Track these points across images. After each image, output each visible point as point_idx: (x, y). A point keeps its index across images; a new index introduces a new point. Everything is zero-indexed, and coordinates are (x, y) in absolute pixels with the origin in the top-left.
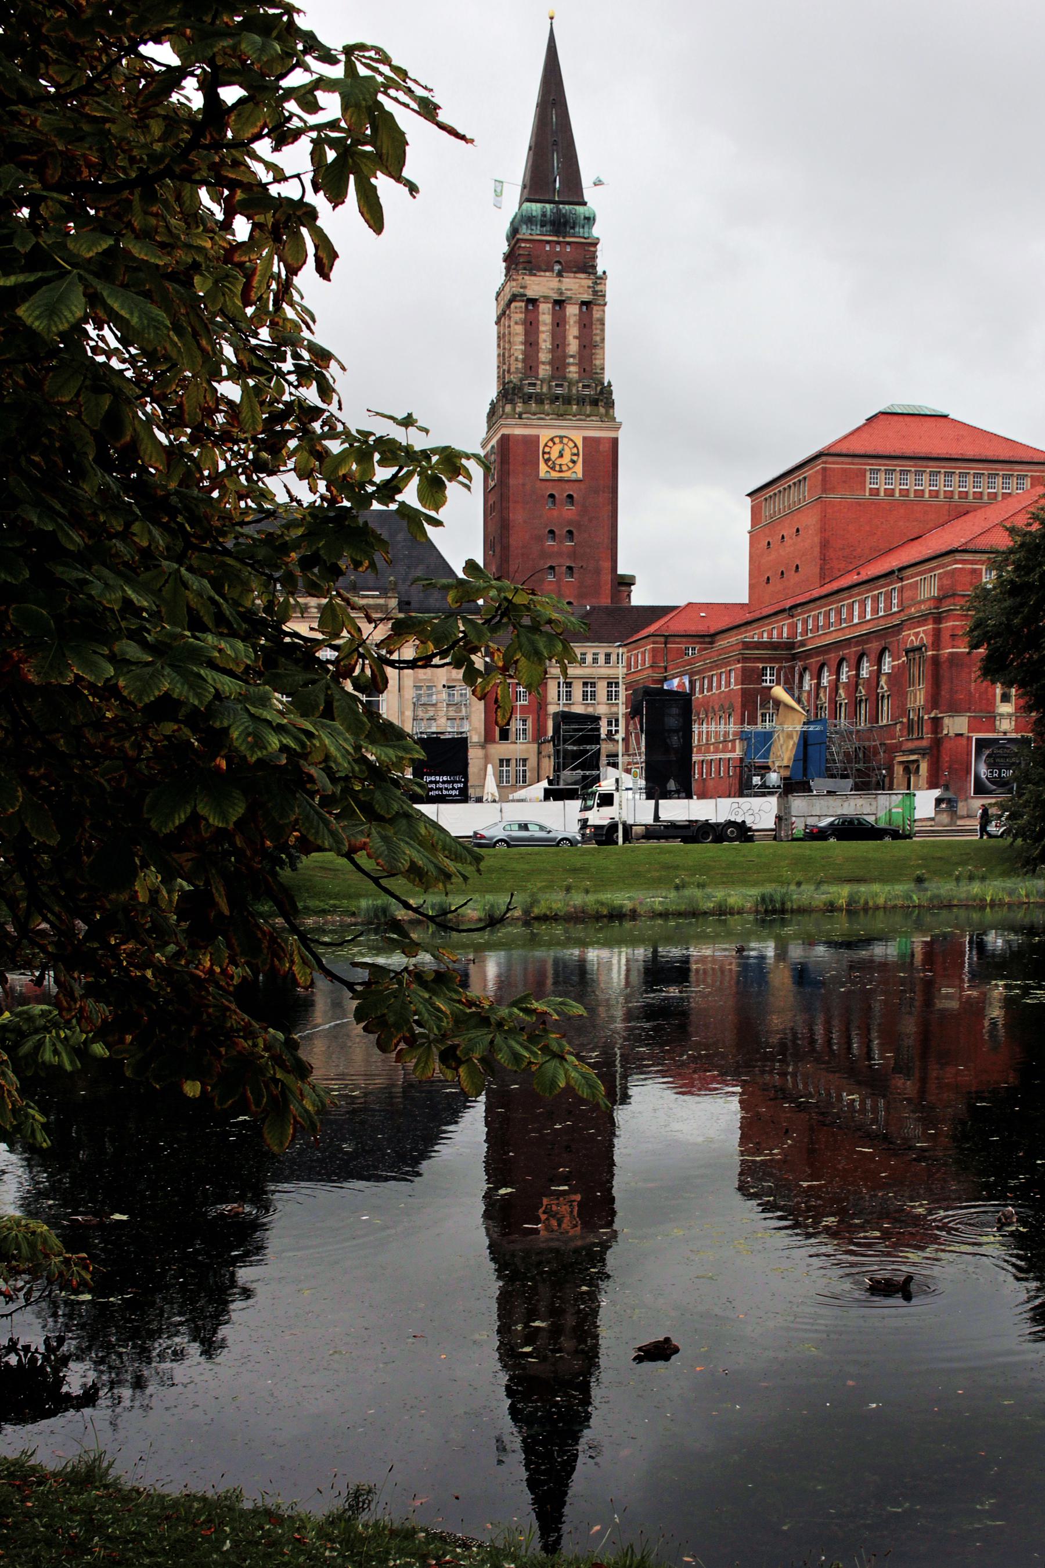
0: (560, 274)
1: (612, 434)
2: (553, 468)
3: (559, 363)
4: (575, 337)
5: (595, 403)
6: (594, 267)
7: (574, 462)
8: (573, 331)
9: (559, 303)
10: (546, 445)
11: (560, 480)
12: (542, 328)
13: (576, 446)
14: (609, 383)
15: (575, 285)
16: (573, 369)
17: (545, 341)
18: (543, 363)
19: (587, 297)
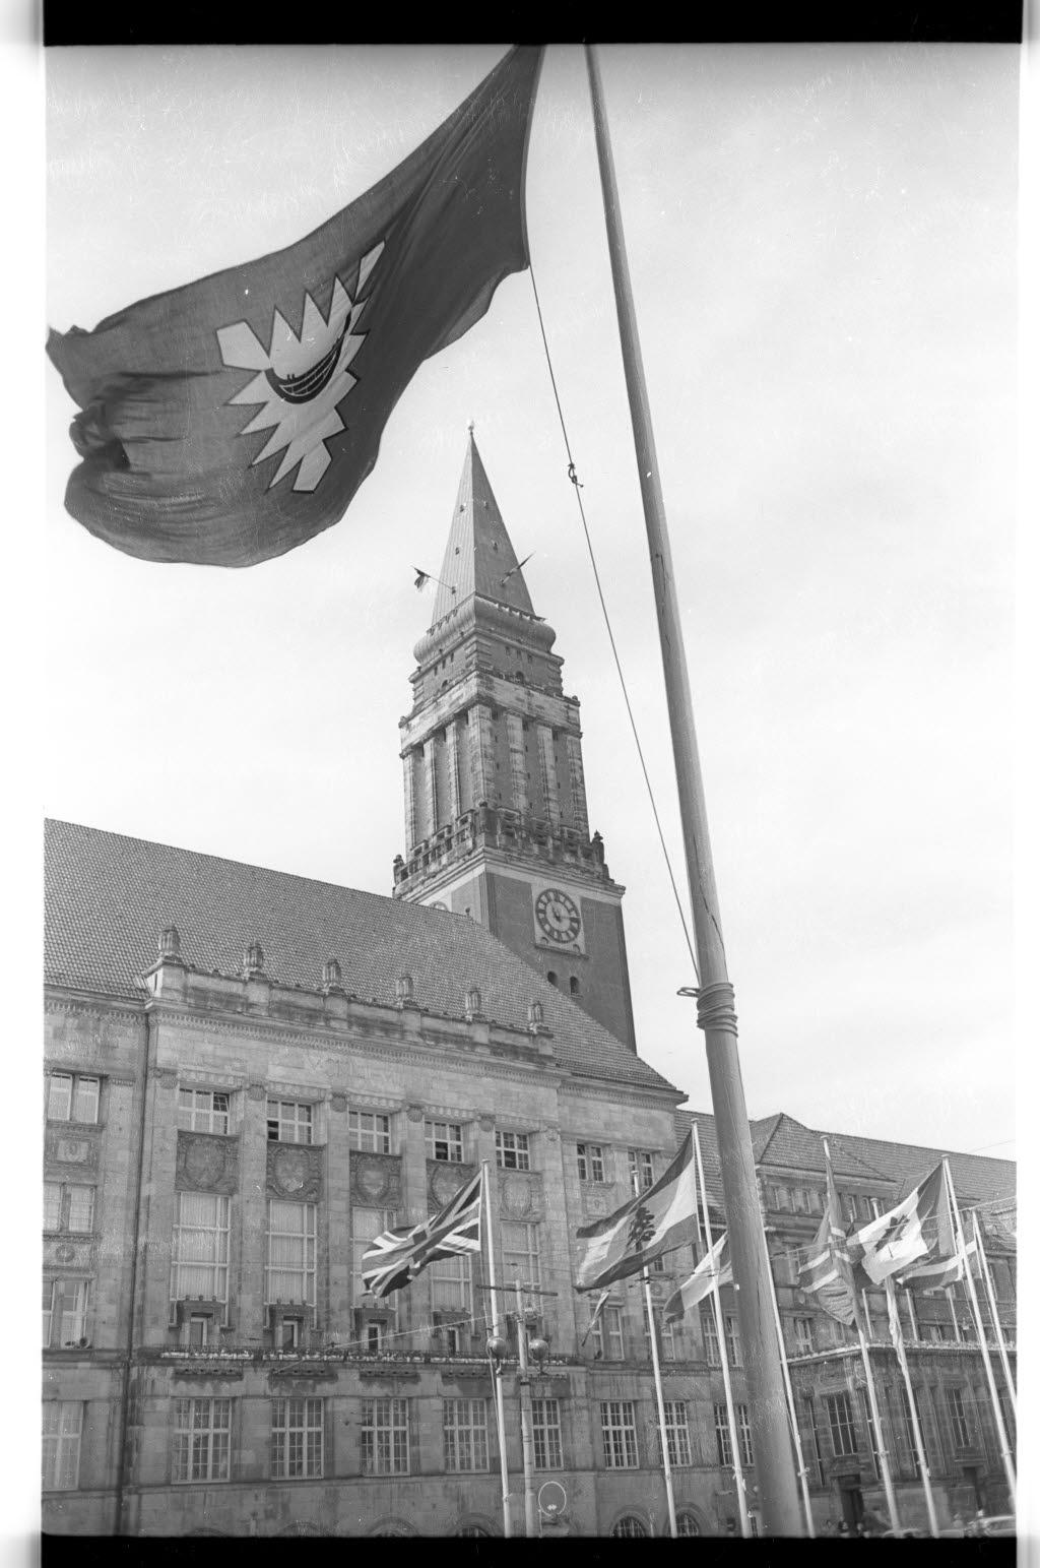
4: (552, 767)
10: (539, 900)
13: (574, 908)
14: (598, 837)
19: (559, 721)
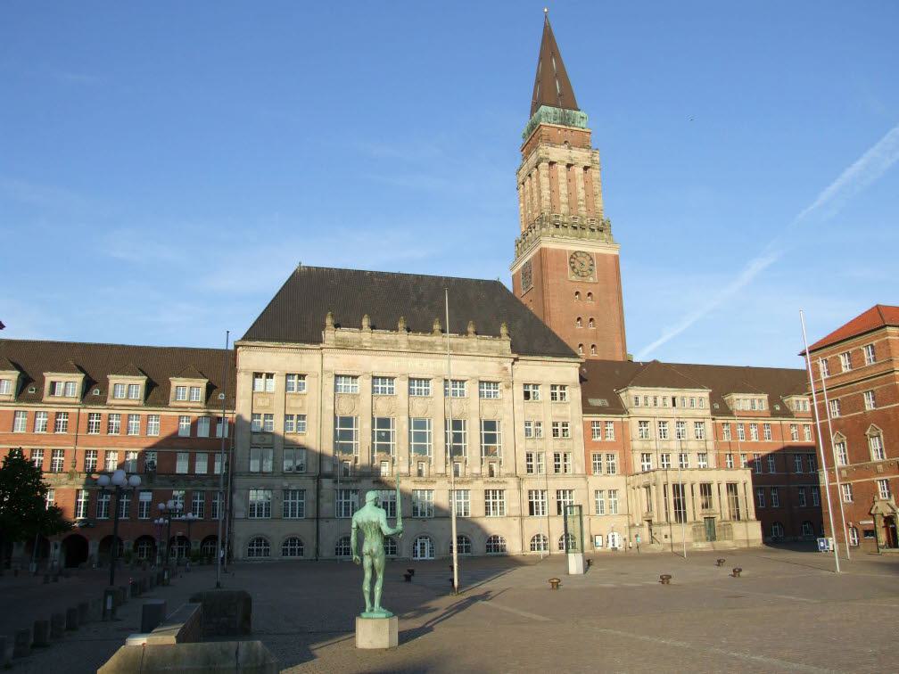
1: (616, 253)
3: (572, 204)
7: (591, 270)
10: (572, 257)
12: (561, 181)
13: (591, 259)
15: (580, 156)
18: (563, 203)
19: (588, 164)
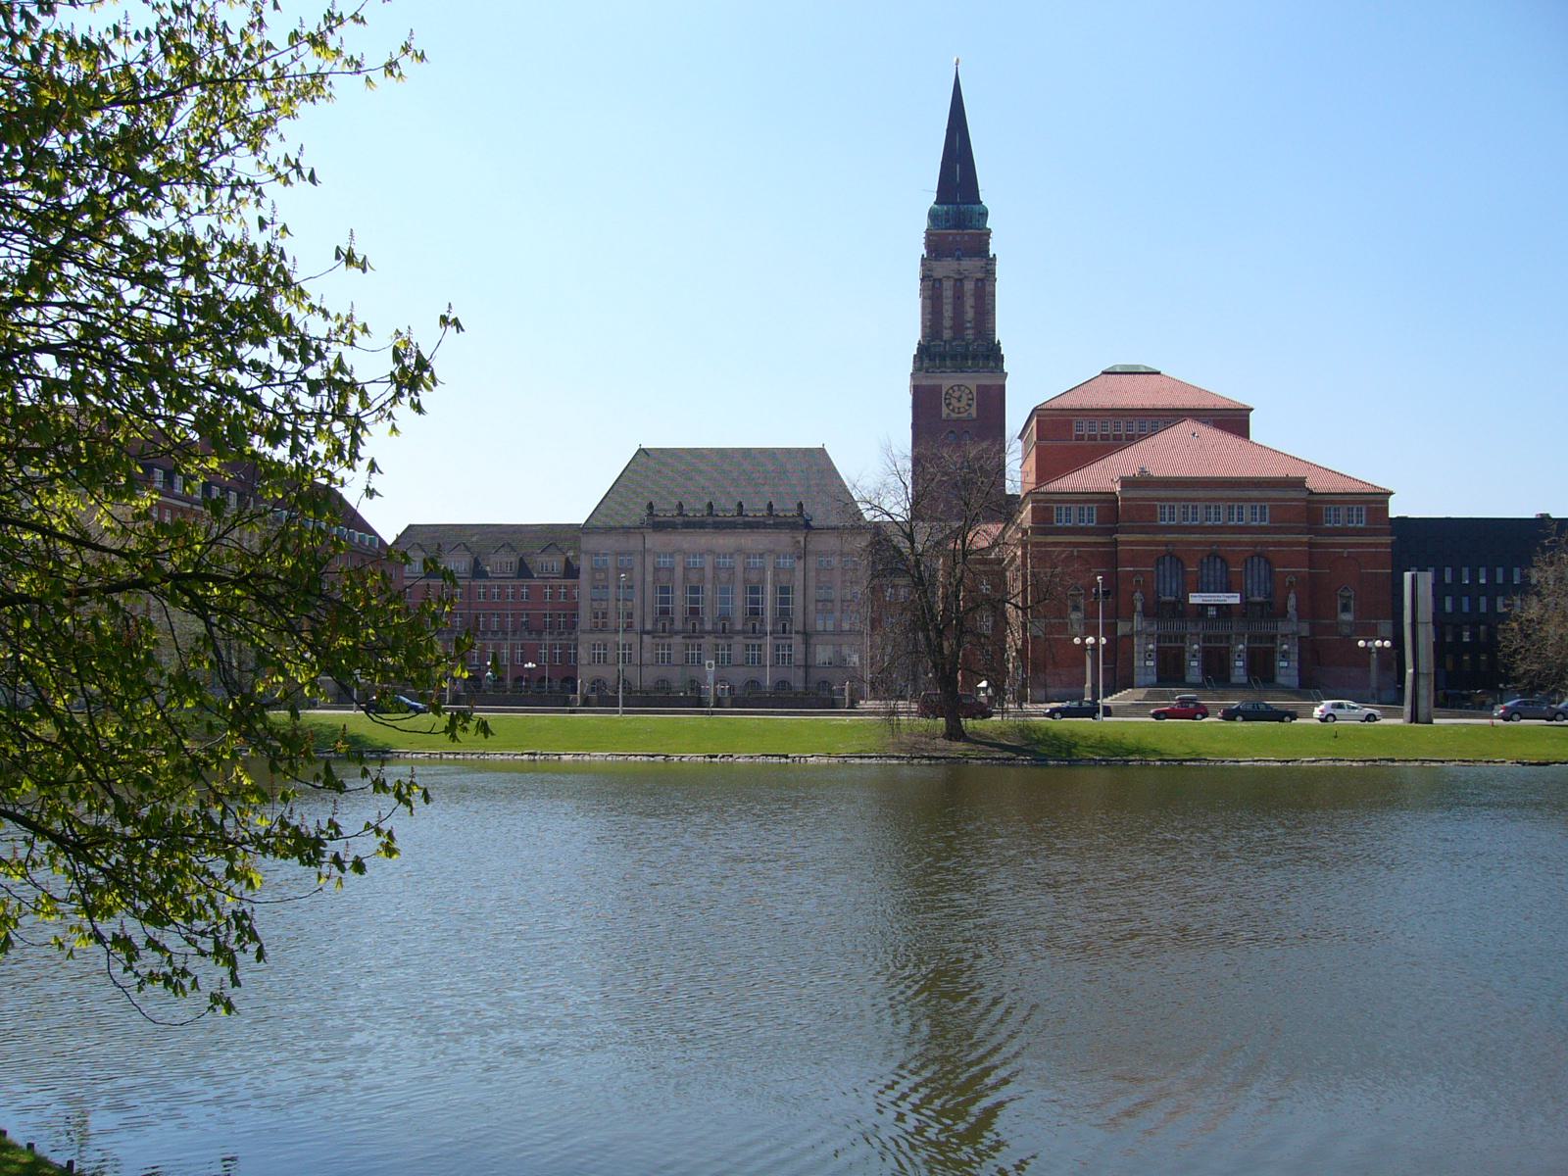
0: (959, 259)
1: (1001, 383)
2: (953, 410)
3: (958, 326)
5: (987, 358)
6: (988, 251)
7: (969, 405)
8: (969, 302)
9: (959, 282)
10: (947, 393)
11: (958, 420)
15: (969, 264)
16: (970, 332)
17: (948, 311)
19: (980, 275)
